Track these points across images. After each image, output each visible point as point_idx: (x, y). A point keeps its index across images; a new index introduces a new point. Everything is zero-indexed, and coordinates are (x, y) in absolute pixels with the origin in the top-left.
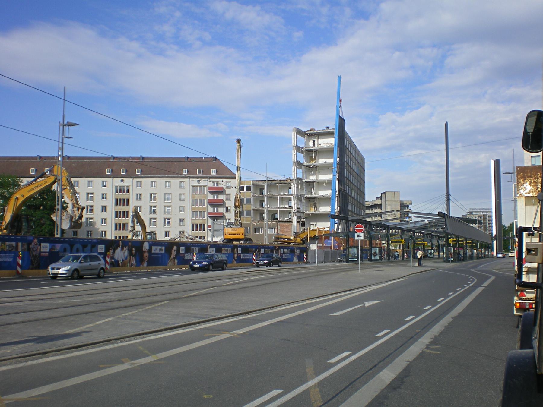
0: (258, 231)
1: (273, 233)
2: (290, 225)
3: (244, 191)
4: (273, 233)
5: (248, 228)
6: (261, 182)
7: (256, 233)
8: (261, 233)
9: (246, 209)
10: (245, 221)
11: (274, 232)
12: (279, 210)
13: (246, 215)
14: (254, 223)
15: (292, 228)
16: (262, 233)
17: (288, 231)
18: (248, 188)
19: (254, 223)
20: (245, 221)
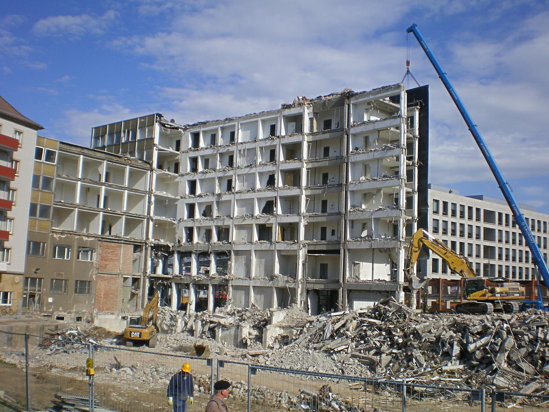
0: (62, 254)
1: (89, 260)
2: (118, 247)
3: (41, 160)
4: (89, 260)
5: (42, 244)
6: (74, 149)
7: (56, 258)
8: (65, 259)
9: (41, 202)
10: (37, 228)
11: (91, 259)
12: (101, 213)
13: (41, 216)
14: (55, 236)
15: (120, 253)
16: (68, 257)
17: (115, 258)
18: (50, 155)
19: (55, 236)
20: (37, 228)
